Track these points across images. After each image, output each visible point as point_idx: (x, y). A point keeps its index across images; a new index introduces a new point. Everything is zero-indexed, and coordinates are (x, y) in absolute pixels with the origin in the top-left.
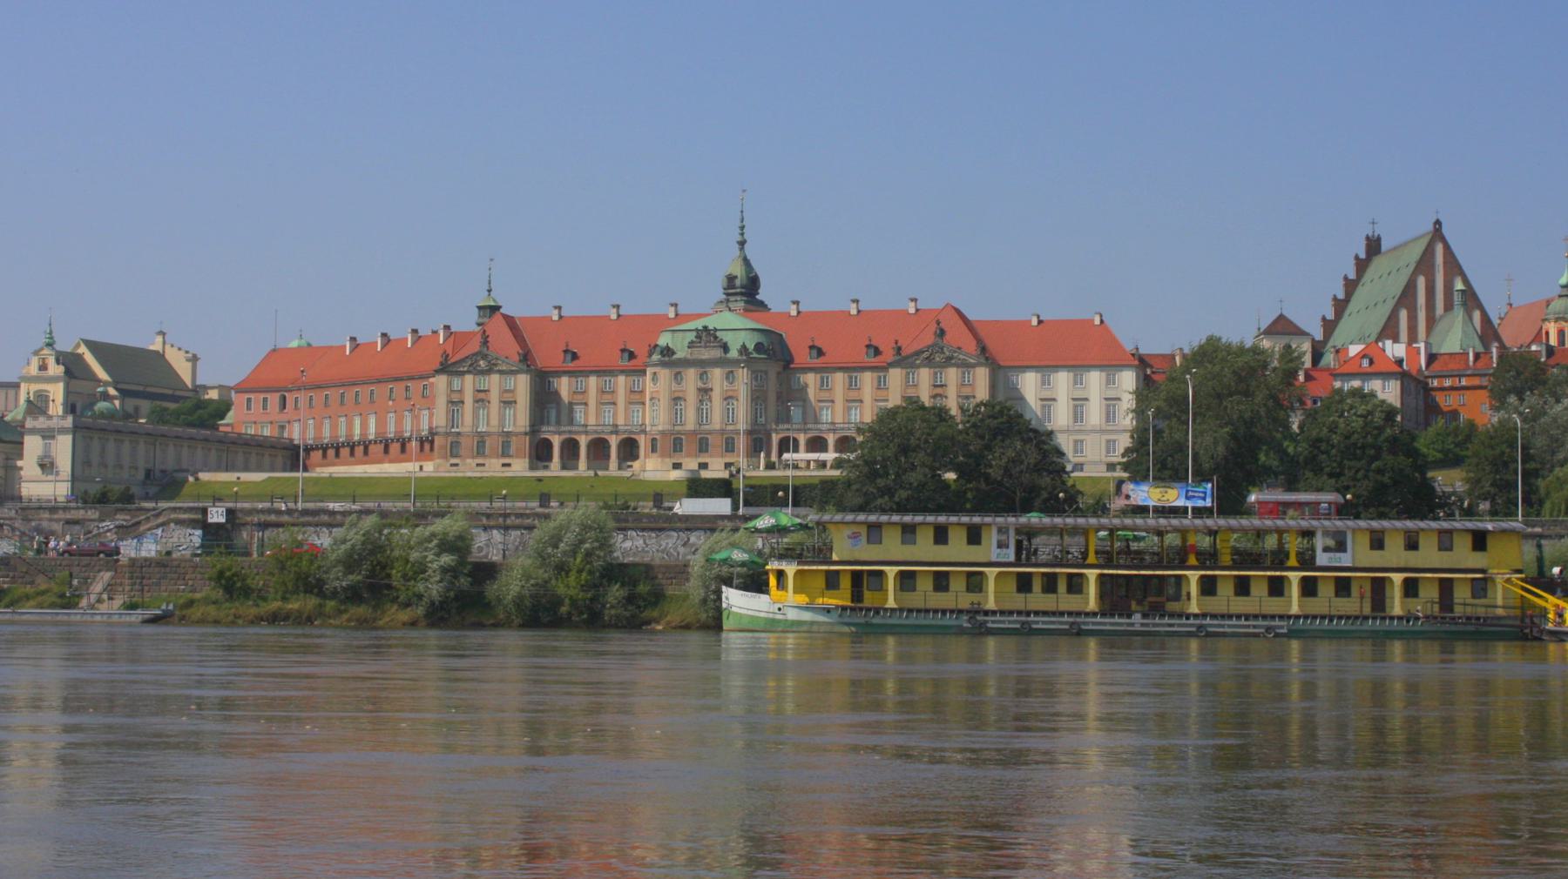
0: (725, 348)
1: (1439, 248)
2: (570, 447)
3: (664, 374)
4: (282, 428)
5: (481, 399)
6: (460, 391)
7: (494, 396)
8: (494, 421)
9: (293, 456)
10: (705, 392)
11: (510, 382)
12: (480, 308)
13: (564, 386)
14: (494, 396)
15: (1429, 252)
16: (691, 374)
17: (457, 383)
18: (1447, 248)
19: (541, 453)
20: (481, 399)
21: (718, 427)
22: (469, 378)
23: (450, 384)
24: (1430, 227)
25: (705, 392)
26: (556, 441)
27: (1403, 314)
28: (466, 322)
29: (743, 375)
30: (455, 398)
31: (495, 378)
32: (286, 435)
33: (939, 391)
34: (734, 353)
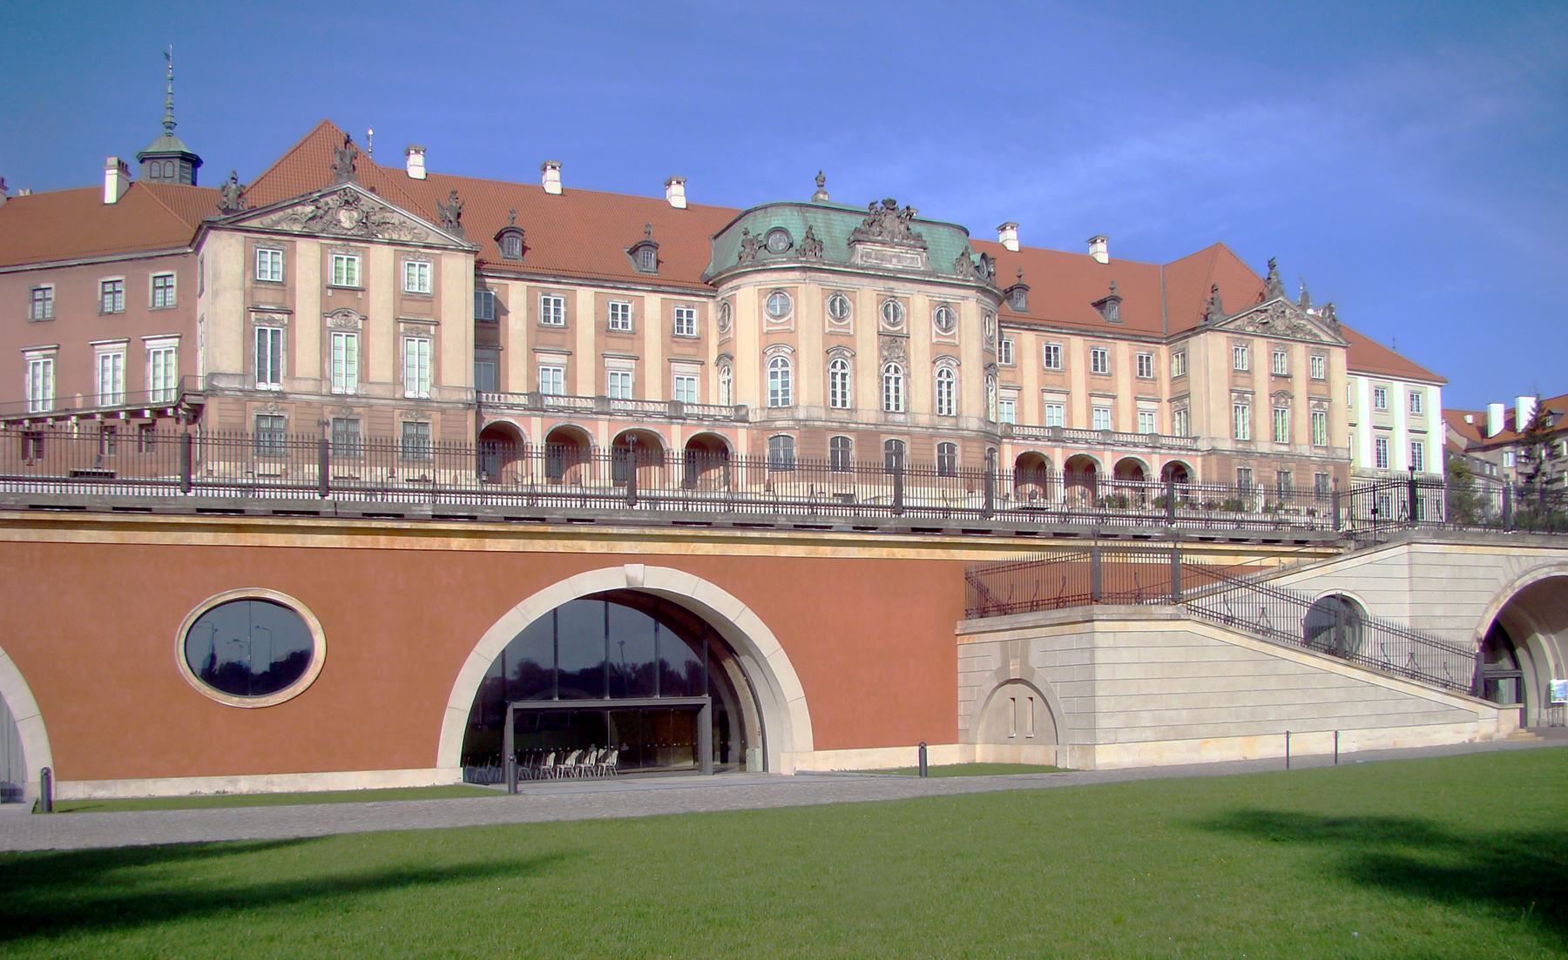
5: (344, 304)
6: (285, 286)
7: (381, 304)
8: (381, 370)
10: (893, 342)
11: (421, 278)
14: (381, 304)
17: (271, 265)
20: (344, 304)
21: (924, 420)
22: (307, 252)
23: (251, 263)
25: (893, 342)
30: (267, 298)
31: (382, 256)
33: (1282, 386)
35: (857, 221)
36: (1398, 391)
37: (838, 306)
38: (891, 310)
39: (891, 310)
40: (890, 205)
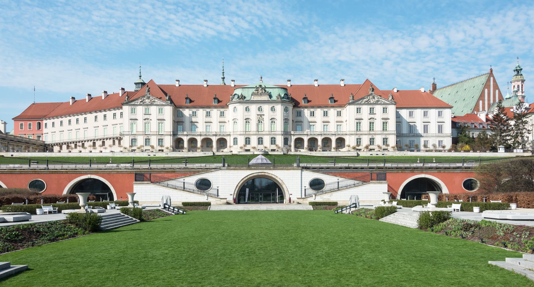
0: (270, 96)
1: (492, 79)
2: (193, 141)
3: (241, 107)
4: (39, 137)
9: (46, 148)
12: (136, 84)
13: (187, 112)
15: (488, 80)
16: (254, 108)
18: (494, 81)
19: (178, 144)
24: (489, 71)
26: (186, 139)
27: (481, 102)
28: (131, 88)
29: (279, 108)
32: (41, 139)
34: (274, 98)
35: (253, 90)
36: (433, 113)
37: (247, 109)
38: (260, 109)
39: (260, 109)
40: (260, 86)
